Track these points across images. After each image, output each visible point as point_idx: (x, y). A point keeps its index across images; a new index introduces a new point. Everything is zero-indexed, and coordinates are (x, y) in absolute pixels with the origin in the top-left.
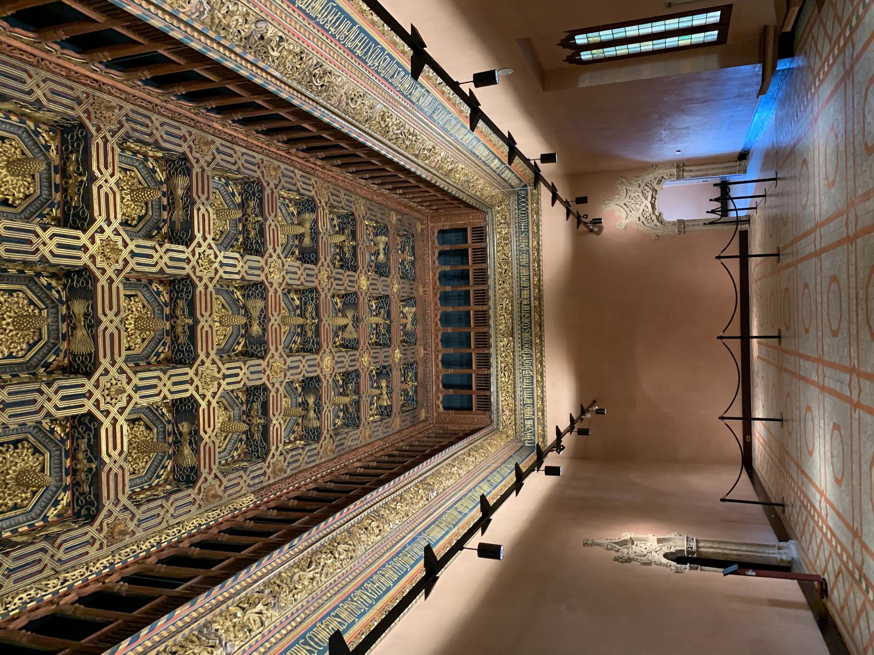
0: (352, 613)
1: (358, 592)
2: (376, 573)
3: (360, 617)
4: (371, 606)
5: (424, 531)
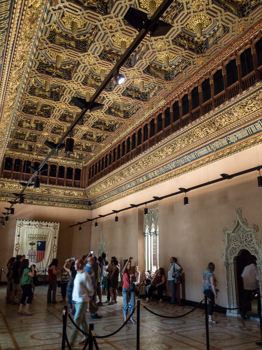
0: (158, 173)
1: (161, 168)
2: (169, 163)
3: (159, 175)
4: (163, 173)
5: (197, 150)
